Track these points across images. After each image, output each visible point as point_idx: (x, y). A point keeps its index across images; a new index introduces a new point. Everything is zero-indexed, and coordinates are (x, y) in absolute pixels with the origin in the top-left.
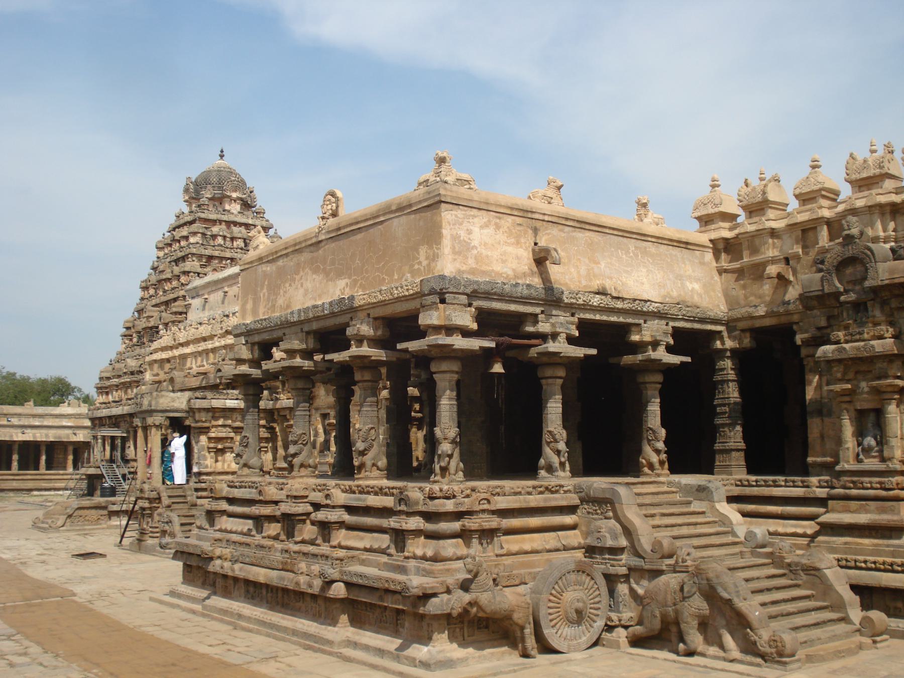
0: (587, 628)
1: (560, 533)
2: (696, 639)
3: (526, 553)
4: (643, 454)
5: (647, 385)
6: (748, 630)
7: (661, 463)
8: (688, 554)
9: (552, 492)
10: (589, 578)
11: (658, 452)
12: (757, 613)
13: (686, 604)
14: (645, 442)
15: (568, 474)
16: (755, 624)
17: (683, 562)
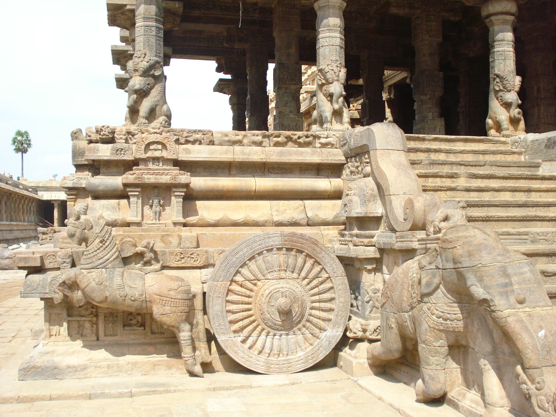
0: (306, 339)
1: (307, 202)
2: (442, 371)
3: (235, 224)
4: (490, 113)
5: (493, 18)
6: (519, 368)
7: (514, 122)
8: (446, 219)
9: (300, 145)
10: (312, 261)
11: (507, 106)
12: (542, 333)
13: (425, 307)
14: (492, 95)
15: (347, 126)
16: (531, 356)
17: (435, 233)
